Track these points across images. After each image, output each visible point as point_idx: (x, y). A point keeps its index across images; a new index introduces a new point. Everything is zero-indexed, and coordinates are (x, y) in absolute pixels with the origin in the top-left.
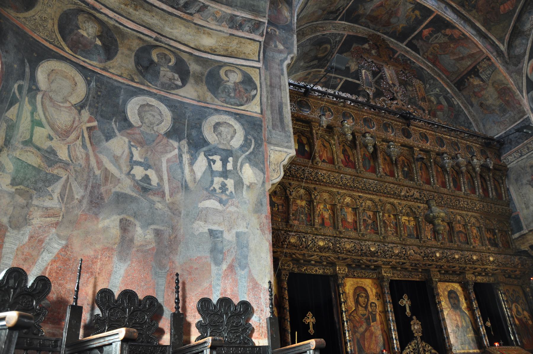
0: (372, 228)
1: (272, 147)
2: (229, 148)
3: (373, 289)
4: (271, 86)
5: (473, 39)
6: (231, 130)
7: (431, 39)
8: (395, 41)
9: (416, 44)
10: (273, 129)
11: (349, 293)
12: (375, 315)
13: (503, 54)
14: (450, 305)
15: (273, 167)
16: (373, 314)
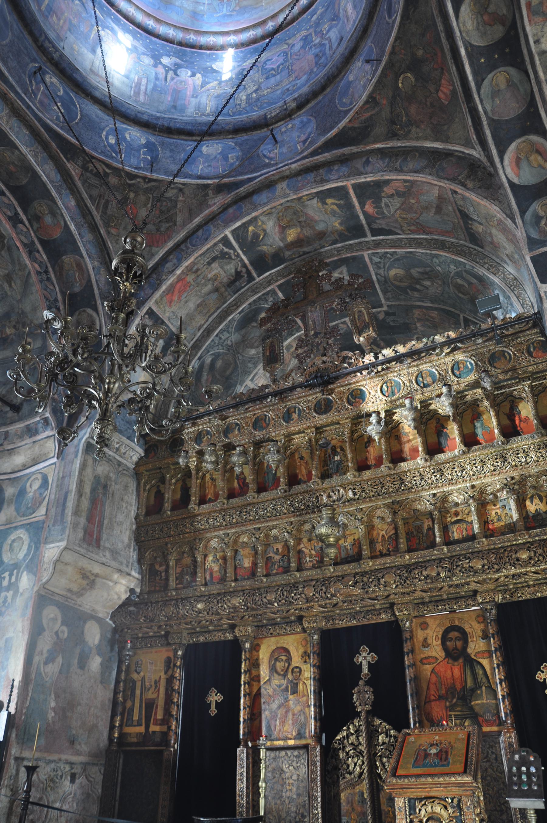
0: (279, 567)
1: (48, 546)
2: (16, 561)
3: (300, 646)
4: (63, 477)
5: (420, 179)
6: (21, 542)
7: (385, 211)
8: (357, 241)
9: (380, 227)
10: (54, 525)
11: (263, 658)
12: (297, 685)
13: (482, 162)
14: (443, 654)
15: (45, 567)
16: (294, 684)
